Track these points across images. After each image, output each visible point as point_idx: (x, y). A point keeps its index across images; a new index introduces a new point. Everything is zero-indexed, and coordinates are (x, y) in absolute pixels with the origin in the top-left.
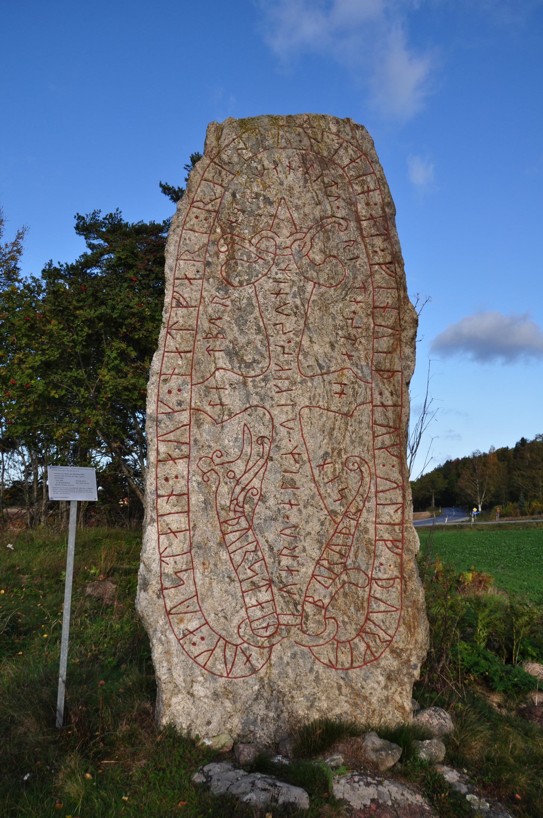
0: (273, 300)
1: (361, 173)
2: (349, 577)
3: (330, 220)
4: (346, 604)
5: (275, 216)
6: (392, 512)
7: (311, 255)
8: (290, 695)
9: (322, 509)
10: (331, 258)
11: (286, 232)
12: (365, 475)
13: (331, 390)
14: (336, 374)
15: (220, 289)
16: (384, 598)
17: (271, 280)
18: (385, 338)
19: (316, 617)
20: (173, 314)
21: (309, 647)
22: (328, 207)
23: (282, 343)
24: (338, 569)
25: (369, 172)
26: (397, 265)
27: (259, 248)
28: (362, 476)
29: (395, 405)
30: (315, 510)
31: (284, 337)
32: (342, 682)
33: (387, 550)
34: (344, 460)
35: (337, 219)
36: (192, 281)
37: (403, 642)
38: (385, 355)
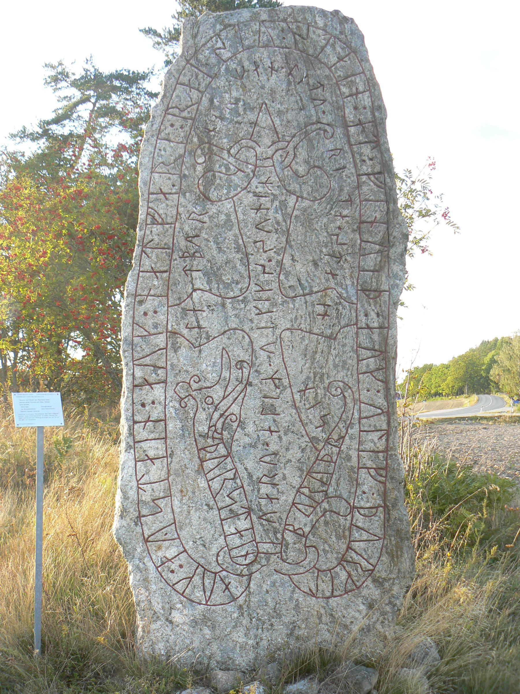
0: (253, 215)
1: (349, 74)
2: (330, 505)
3: (314, 127)
4: (326, 532)
5: (256, 124)
6: (376, 440)
7: (294, 166)
8: (269, 623)
9: (303, 436)
10: (316, 169)
11: (267, 141)
12: (349, 400)
13: (313, 311)
14: (320, 294)
15: (197, 204)
16: (366, 527)
17: (251, 195)
18: (372, 255)
19: (297, 546)
20: (148, 232)
21: (289, 575)
22: (313, 112)
23: (262, 262)
24: (319, 497)
25: (358, 72)
26: (386, 175)
27: (238, 159)
28: (346, 402)
29: (380, 328)
30: (296, 437)
31: (265, 256)
32: (323, 611)
33: (370, 478)
34: (326, 385)
35: (322, 126)
36: (167, 196)
37: (386, 571)
38: (372, 273)
